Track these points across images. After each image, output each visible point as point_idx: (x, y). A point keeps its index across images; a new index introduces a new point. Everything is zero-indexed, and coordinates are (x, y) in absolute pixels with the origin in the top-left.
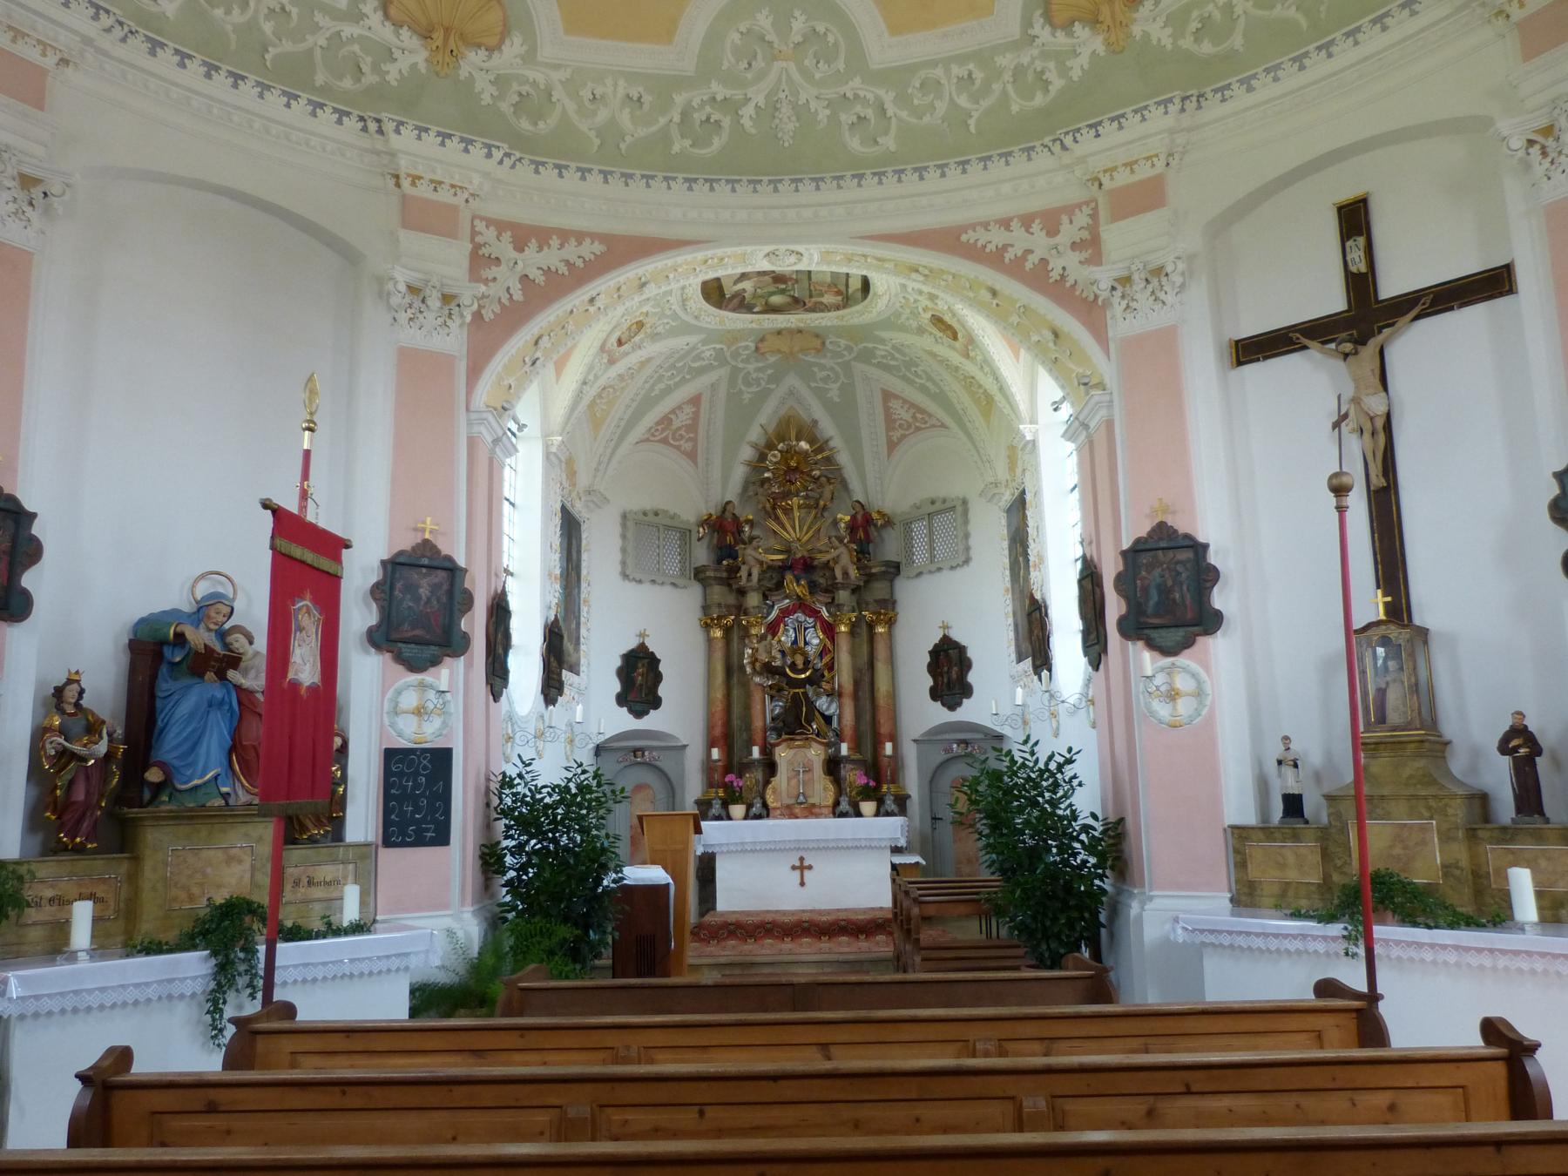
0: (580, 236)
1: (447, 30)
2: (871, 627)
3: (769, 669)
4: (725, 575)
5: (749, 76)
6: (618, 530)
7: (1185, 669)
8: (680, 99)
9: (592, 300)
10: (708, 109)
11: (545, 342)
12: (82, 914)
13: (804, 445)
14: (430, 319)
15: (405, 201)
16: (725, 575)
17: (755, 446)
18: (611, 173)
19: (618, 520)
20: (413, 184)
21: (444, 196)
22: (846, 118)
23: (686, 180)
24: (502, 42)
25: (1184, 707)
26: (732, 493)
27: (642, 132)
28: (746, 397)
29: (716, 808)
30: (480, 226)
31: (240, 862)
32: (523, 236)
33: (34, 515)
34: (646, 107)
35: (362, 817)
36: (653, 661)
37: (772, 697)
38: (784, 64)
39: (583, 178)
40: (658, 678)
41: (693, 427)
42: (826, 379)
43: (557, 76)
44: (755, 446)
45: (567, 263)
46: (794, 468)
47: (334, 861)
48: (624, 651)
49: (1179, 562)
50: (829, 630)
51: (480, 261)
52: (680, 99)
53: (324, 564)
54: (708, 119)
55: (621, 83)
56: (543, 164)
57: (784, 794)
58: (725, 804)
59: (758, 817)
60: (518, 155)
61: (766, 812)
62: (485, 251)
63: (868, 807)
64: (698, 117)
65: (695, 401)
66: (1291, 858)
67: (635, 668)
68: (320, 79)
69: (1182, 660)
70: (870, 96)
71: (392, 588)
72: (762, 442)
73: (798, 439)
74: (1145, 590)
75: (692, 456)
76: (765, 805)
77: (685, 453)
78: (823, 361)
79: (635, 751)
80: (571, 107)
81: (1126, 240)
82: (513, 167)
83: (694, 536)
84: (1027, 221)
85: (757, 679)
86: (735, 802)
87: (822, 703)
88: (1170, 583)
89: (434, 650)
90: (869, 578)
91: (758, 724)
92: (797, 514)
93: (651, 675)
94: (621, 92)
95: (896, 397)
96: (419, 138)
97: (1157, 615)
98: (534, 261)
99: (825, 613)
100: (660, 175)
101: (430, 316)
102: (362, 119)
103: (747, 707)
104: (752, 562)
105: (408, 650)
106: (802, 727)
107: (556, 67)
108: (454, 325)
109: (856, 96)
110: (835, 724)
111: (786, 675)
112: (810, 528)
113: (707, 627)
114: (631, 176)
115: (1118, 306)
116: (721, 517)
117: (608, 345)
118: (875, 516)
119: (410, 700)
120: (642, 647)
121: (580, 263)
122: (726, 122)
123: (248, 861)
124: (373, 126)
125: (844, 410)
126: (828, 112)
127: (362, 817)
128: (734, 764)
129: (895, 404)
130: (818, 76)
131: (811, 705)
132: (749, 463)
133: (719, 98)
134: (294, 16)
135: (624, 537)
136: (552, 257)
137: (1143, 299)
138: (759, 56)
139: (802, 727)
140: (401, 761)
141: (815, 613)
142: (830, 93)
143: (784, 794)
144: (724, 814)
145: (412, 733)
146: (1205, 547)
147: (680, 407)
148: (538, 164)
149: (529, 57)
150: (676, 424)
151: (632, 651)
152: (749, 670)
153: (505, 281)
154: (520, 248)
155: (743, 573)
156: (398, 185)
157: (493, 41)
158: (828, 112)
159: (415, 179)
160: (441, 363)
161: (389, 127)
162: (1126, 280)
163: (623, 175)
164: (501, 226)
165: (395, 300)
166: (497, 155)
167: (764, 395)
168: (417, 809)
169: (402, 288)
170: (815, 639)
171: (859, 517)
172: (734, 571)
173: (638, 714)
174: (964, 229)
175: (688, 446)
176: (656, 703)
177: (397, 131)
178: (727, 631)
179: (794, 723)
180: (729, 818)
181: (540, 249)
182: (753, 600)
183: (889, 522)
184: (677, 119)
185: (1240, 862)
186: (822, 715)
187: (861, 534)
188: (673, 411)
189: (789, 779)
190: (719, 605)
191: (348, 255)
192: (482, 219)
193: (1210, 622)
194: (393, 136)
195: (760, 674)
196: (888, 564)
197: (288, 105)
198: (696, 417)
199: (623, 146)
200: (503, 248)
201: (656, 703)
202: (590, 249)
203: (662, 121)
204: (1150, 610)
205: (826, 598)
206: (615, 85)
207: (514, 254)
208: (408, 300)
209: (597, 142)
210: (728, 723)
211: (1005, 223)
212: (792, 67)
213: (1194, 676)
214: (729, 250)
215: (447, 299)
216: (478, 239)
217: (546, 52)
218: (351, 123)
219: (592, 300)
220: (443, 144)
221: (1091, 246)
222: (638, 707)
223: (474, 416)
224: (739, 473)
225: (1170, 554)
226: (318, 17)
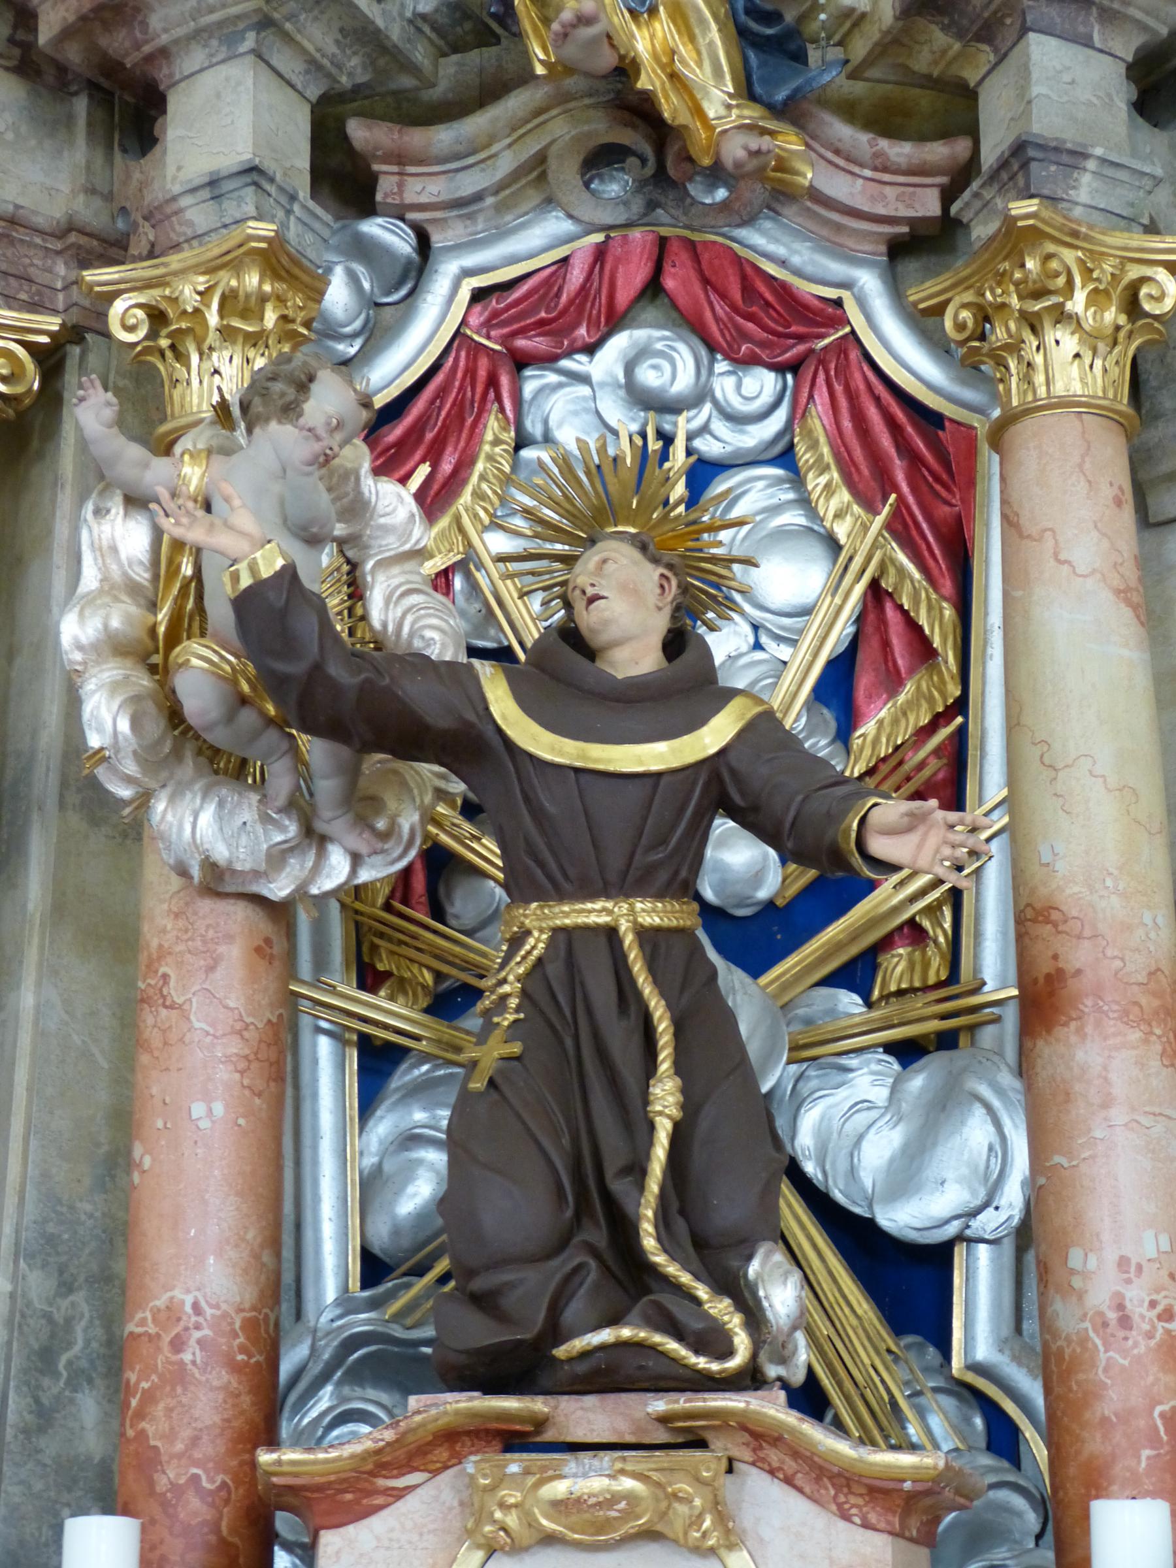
3: (314, 690)
37: (378, 1060)
50: (926, 474)
85: (200, 823)
87: (851, 1121)
91: (198, 1276)
106: (633, 1281)
110: (978, 1319)
111: (470, 747)
131: (738, 1129)
141: (786, 330)
195: (228, 767)
205: (870, 177)
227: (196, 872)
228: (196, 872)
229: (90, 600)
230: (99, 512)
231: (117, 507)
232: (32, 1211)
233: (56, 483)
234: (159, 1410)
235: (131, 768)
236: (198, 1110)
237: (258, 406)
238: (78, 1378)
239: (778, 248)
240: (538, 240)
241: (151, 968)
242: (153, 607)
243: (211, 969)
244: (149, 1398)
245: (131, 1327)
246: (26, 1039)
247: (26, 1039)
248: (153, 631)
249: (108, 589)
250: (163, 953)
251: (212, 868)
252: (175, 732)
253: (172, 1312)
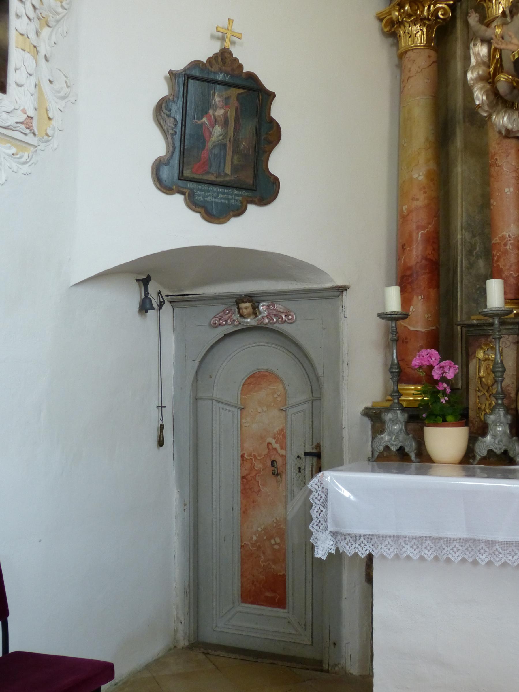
29: (395, 433)
36: (254, 97)
40: (268, 134)
48: (180, 64)
58: (419, 418)
67: (205, 107)
79: (240, 299)
85: (503, 120)
86: (440, 419)
93: (249, 127)
103: (485, 202)
113: (392, 29)
120: (224, 57)
144: (411, 448)
151: (196, 64)
152: (480, 96)
176: (263, 189)
201: (263, 189)
210: (439, 240)
222: (214, 196)
227: (503, 132)
228: (503, 132)
229: (474, 67)
230: (475, 45)
231: (479, 44)
232: (464, 218)
233: (456, 40)
234: (502, 260)
235: (486, 108)
236: (507, 190)
237: (514, 10)
238: (478, 256)
241: (492, 157)
242: (489, 67)
243: (507, 156)
244: (499, 257)
245: (494, 242)
246: (459, 179)
247: (459, 179)
248: (490, 73)
249: (478, 64)
250: (495, 154)
251: (508, 131)
253: (503, 237)
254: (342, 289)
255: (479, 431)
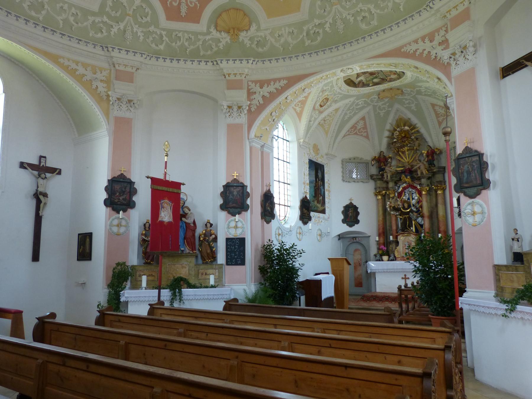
0: (279, 80)
1: (234, 29)
2: (436, 191)
3: (395, 209)
4: (380, 177)
5: (326, 14)
6: (340, 165)
7: (478, 204)
8: (305, 28)
9: (286, 98)
10: (315, 29)
11: (274, 114)
12: (144, 279)
13: (407, 128)
14: (235, 114)
15: (228, 81)
16: (380, 177)
17: (389, 131)
18: (285, 58)
19: (341, 162)
20: (229, 76)
21: (238, 77)
22: (359, 18)
23: (309, 54)
24: (250, 27)
25: (478, 218)
26: (384, 148)
27: (295, 42)
28: (382, 114)
30: (250, 83)
31: (185, 268)
32: (262, 83)
33: (134, 183)
34: (295, 34)
35: (221, 258)
36: (355, 208)
38: (336, 7)
39: (277, 62)
40: (358, 214)
41: (365, 127)
42: (409, 103)
43: (269, 31)
44: (389, 131)
45: (276, 89)
46: (405, 136)
47: (213, 269)
49: (473, 162)
50: (420, 194)
51: (250, 93)
52: (305, 28)
53: (175, 191)
54: (315, 32)
55: (287, 28)
56: (265, 60)
57: (402, 253)
58: (381, 255)
59: (392, 260)
60: (257, 60)
61: (395, 259)
62: (251, 91)
63: (385, 258)
64: (312, 32)
65: (363, 119)
66: (515, 279)
67: (348, 211)
68: (202, 53)
69: (477, 200)
70: (366, 9)
71: (226, 193)
72: (392, 129)
73: (404, 126)
74: (462, 173)
75: (367, 137)
76: (395, 256)
77: (364, 137)
78: (405, 97)
79: (353, 238)
80: (273, 40)
81: (455, 37)
82: (256, 64)
83: (370, 165)
84: (423, 39)
85: (392, 213)
86: (384, 255)
88: (471, 170)
89: (239, 210)
90: (434, 174)
92: (407, 153)
94: (287, 31)
95: (437, 105)
96: (227, 63)
97: (467, 183)
98: (266, 90)
99: (419, 187)
100: (300, 54)
101: (235, 114)
102: (212, 62)
104: (388, 172)
105: (231, 210)
106: (407, 229)
107: (266, 30)
108: (243, 115)
109: (361, 10)
112: (412, 157)
113: (376, 195)
114: (292, 57)
115: (453, 63)
116: (379, 157)
117: (316, 108)
118: (436, 150)
119: (233, 224)
120: (351, 203)
121: (280, 88)
122: (321, 31)
123: (187, 268)
124: (215, 63)
125: (419, 113)
126: (353, 18)
127: (221, 258)
128: (387, 243)
129: (437, 108)
130: (347, 7)
132: (388, 137)
133: (317, 24)
134: (193, 39)
135: (343, 168)
136: (272, 88)
137: (461, 60)
138: (327, 5)
139: (407, 229)
140: (231, 241)
141: (415, 188)
142: (352, 12)
143: (402, 253)
145: (233, 233)
146: (483, 154)
147: (358, 122)
148: (263, 61)
149: (258, 29)
150: (359, 128)
151: (347, 205)
152: (389, 209)
153: (258, 99)
154: (261, 87)
155: (385, 176)
156: (225, 77)
157: (247, 28)
158: (353, 18)
159: (229, 75)
160: (239, 127)
161: (219, 62)
162: (454, 54)
163: (289, 57)
164: (256, 82)
165: (224, 111)
166: (251, 62)
167: (388, 113)
168: (236, 255)
169: (225, 107)
170: (416, 196)
171: (430, 151)
172: (382, 175)
173: (351, 226)
174: (402, 47)
175: (365, 134)
176: (357, 222)
177: (221, 62)
178: (384, 196)
179: (405, 228)
180: (382, 260)
181: (268, 86)
182: (391, 185)
183: (441, 152)
184: (305, 35)
185: (498, 279)
186: (419, 224)
187: (430, 157)
188: (356, 124)
189: (403, 247)
190: (379, 188)
191: (215, 101)
192: (250, 81)
193: (485, 184)
194: (220, 64)
195: (393, 211)
196: (440, 168)
197: (192, 64)
198: (365, 124)
199: (290, 48)
200: (257, 89)
201: (357, 222)
202: (283, 83)
203: (301, 37)
204: (464, 181)
206: (285, 30)
207: (260, 90)
208: (228, 110)
209: (282, 49)
210: (383, 228)
211: (416, 41)
212: (339, 6)
213: (481, 206)
214: (327, 73)
215: (240, 107)
216: (249, 88)
217: (263, 26)
218: (210, 64)
219: (286, 98)
220: (234, 63)
221: (445, 43)
222: (351, 224)
223: (250, 140)
224: (385, 141)
225: (470, 159)
226: (200, 37)
239: (415, 185)
240: (405, 185)
252: (391, 210)
254: (370, 236)
255: (389, 257)
